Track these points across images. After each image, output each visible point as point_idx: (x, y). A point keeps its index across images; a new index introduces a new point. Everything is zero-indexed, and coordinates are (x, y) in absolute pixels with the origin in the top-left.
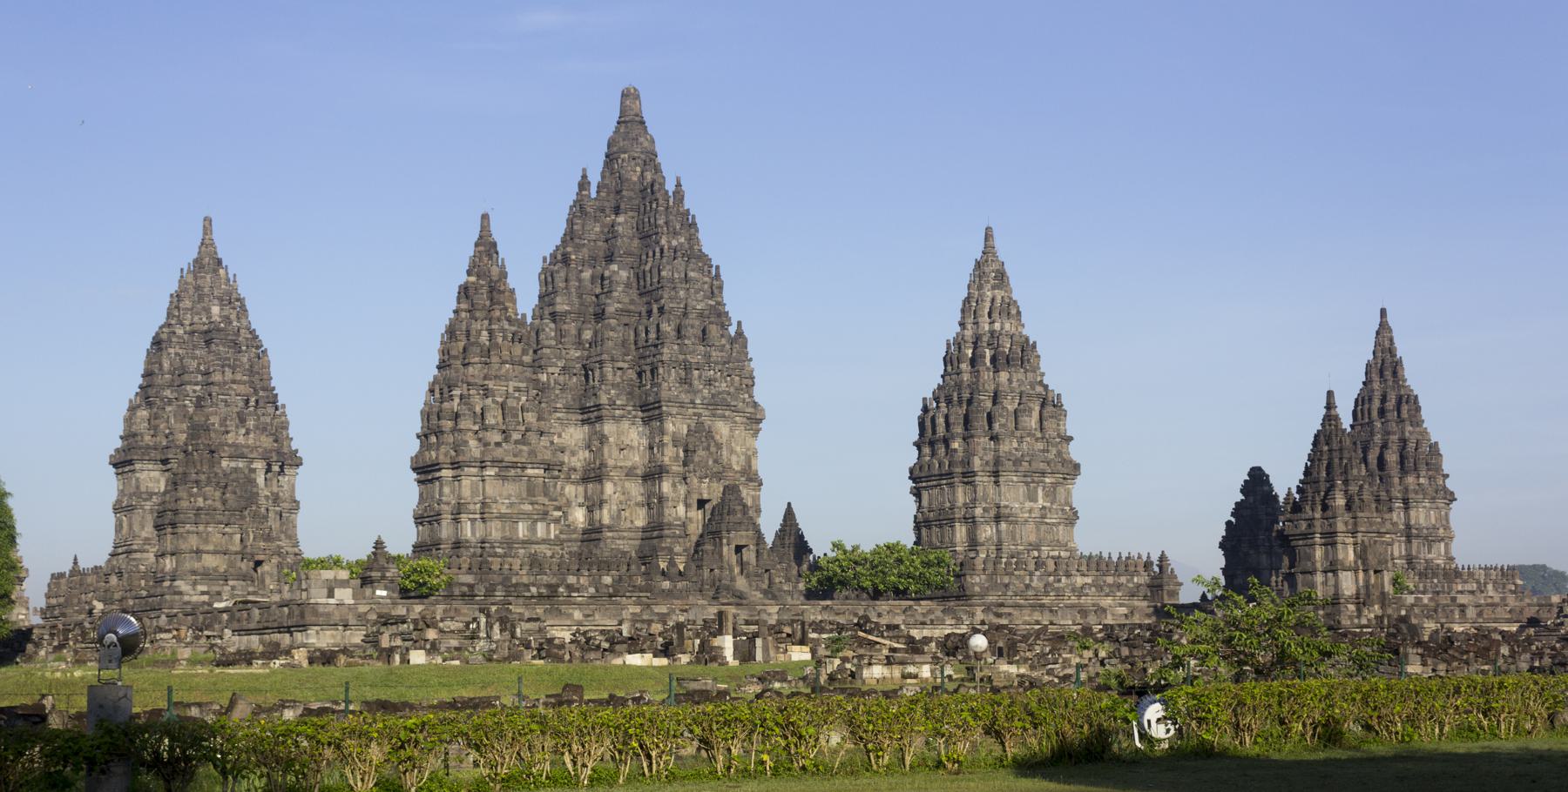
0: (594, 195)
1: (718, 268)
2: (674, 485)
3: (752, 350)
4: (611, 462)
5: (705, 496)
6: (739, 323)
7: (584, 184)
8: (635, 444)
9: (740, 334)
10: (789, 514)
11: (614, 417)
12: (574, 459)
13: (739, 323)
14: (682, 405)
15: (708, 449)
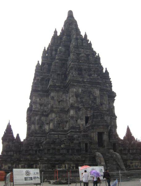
0: (59, 34)
1: (98, 54)
2: (76, 112)
3: (111, 76)
4: (54, 106)
5: (89, 115)
6: (106, 69)
7: (56, 32)
8: (65, 99)
9: (106, 71)
10: (128, 130)
11: (56, 90)
12: (45, 108)
13: (106, 69)
14: (78, 82)
15: (89, 96)
